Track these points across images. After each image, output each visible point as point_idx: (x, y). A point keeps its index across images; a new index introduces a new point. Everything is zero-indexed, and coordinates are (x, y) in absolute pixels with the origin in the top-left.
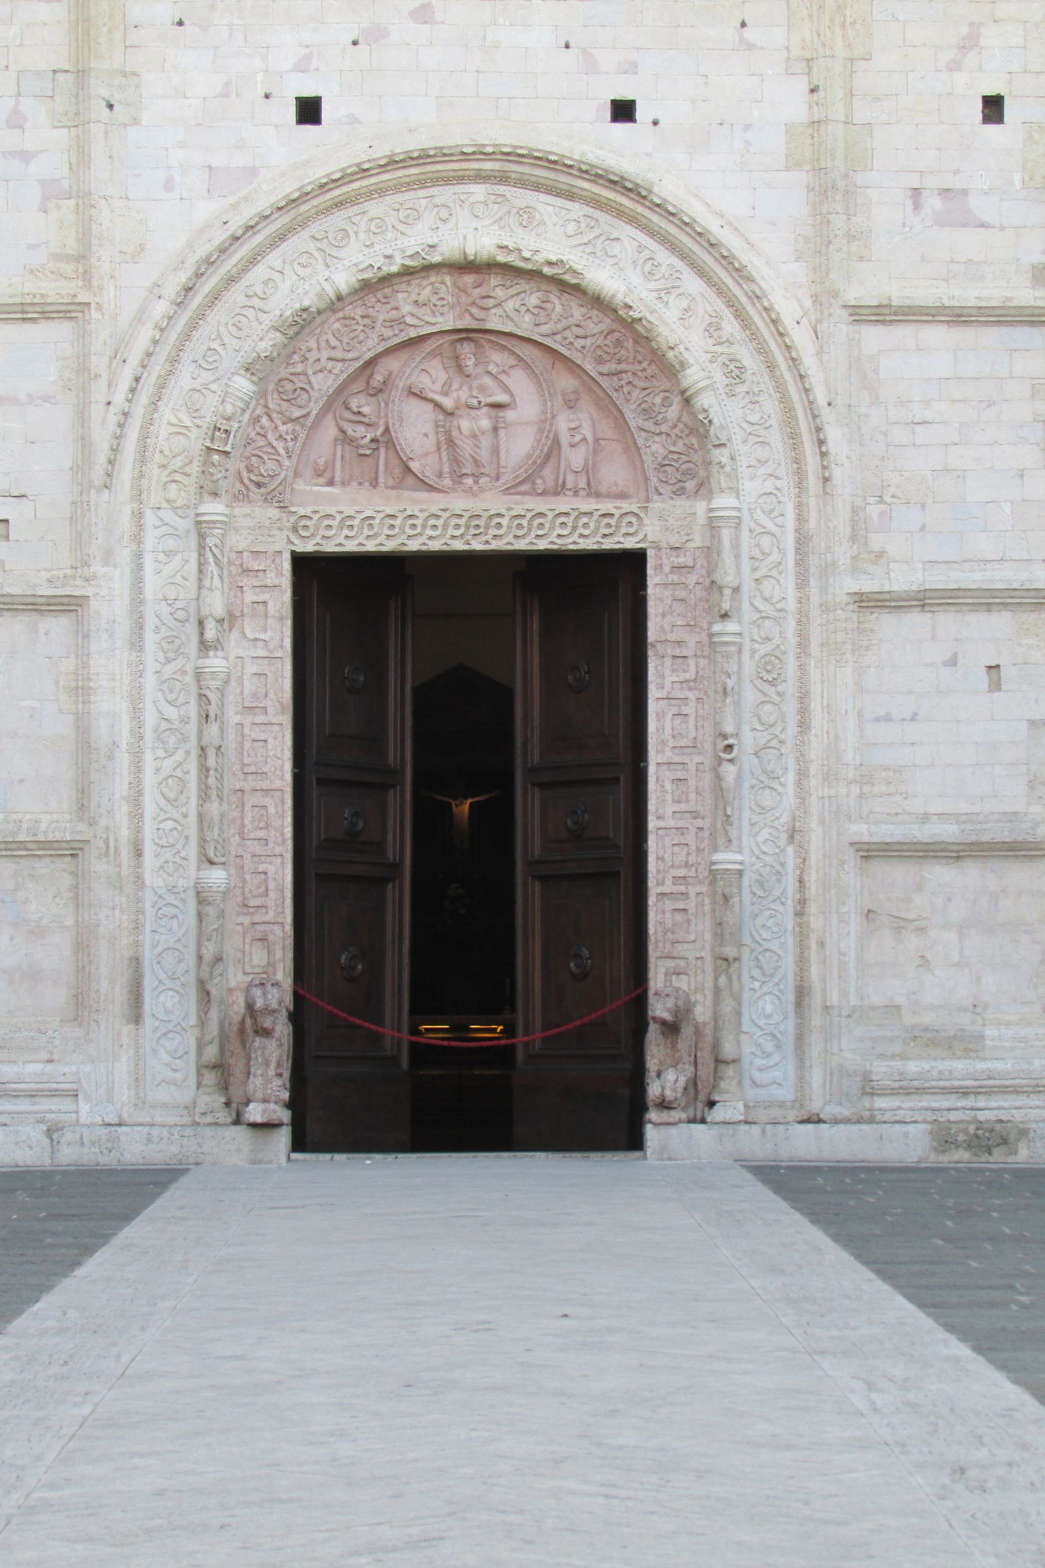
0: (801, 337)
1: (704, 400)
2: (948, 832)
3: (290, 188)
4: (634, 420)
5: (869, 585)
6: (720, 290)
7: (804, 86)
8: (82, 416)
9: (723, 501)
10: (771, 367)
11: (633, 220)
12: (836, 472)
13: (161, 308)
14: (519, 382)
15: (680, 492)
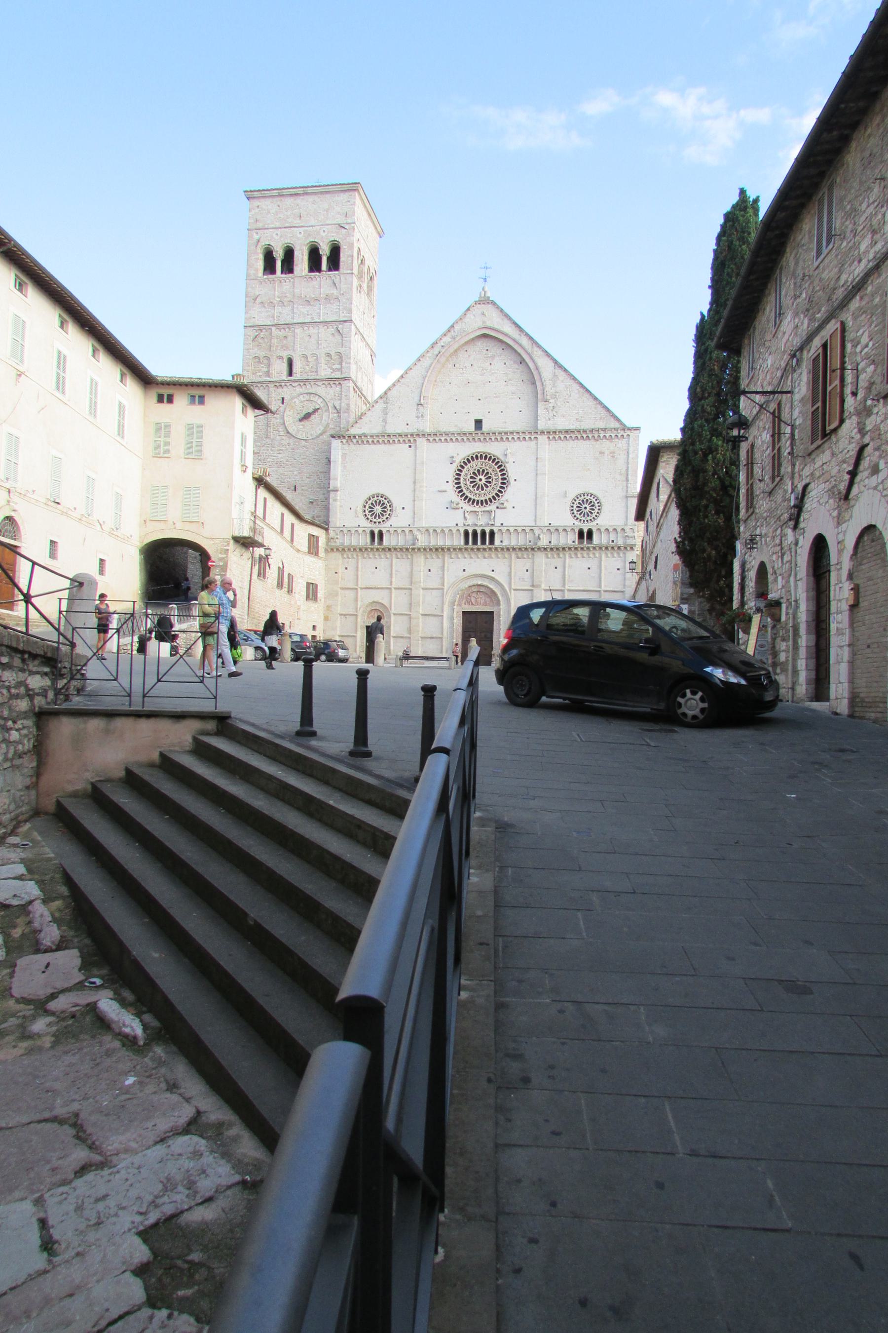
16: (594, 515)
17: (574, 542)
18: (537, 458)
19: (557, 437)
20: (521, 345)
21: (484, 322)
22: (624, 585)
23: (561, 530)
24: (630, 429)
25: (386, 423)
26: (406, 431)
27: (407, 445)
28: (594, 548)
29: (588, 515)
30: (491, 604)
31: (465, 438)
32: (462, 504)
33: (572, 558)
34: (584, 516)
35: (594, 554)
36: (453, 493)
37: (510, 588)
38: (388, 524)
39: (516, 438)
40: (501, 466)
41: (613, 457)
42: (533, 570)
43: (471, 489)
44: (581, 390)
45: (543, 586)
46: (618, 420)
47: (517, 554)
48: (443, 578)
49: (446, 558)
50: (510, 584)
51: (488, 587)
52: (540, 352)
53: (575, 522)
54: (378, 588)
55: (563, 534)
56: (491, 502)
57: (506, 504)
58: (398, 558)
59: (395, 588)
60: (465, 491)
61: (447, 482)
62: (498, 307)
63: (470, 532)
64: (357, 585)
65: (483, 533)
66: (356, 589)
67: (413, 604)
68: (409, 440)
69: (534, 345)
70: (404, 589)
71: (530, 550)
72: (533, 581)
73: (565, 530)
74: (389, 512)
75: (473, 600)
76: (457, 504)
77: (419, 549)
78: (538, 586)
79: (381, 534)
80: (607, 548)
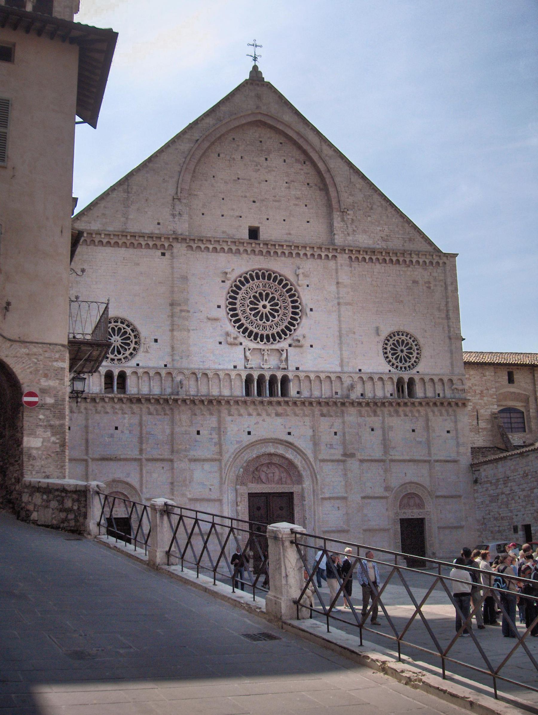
0: (313, 464)
1: (302, 472)
2: (334, 529)
3: (248, 443)
4: (292, 475)
5: (323, 496)
6: (303, 458)
7: (312, 430)
8: (221, 474)
9: (304, 486)
10: (309, 467)
11: (291, 448)
12: (319, 482)
13: (231, 459)
14: (276, 469)
15: (298, 484)
16: (413, 360)
17: (391, 395)
18: (338, 283)
19: (360, 257)
20: (306, 141)
21: (258, 107)
22: (458, 453)
23: (376, 377)
24: (446, 255)
25: (127, 218)
26: (157, 232)
27: (159, 253)
28: (420, 404)
29: (406, 361)
30: (289, 481)
31: (242, 249)
32: (241, 339)
33: (393, 416)
34: (401, 362)
35: (418, 411)
36: (227, 322)
37: (316, 458)
38: (133, 363)
39: (309, 254)
40: (291, 290)
41: (429, 288)
42: (344, 434)
43: (252, 318)
44: (383, 203)
45: (359, 456)
46: (431, 243)
47: (321, 410)
48: (220, 444)
49: (223, 415)
50: (315, 452)
51: (282, 457)
52: (331, 152)
53: (391, 368)
54: (120, 460)
55: (379, 384)
56: (280, 338)
57: (302, 342)
58: (150, 414)
59: (148, 460)
60: (243, 321)
61: (219, 307)
62: (276, 91)
63: (256, 377)
64: (87, 454)
65: (273, 378)
66: (86, 460)
67: (175, 483)
68: (163, 246)
69: (323, 143)
70: (162, 460)
71: (339, 404)
72: (345, 448)
73: (381, 379)
74: (133, 345)
75: (263, 477)
76: (235, 338)
77: (184, 401)
78: (352, 455)
79: (122, 376)
80: (435, 404)
